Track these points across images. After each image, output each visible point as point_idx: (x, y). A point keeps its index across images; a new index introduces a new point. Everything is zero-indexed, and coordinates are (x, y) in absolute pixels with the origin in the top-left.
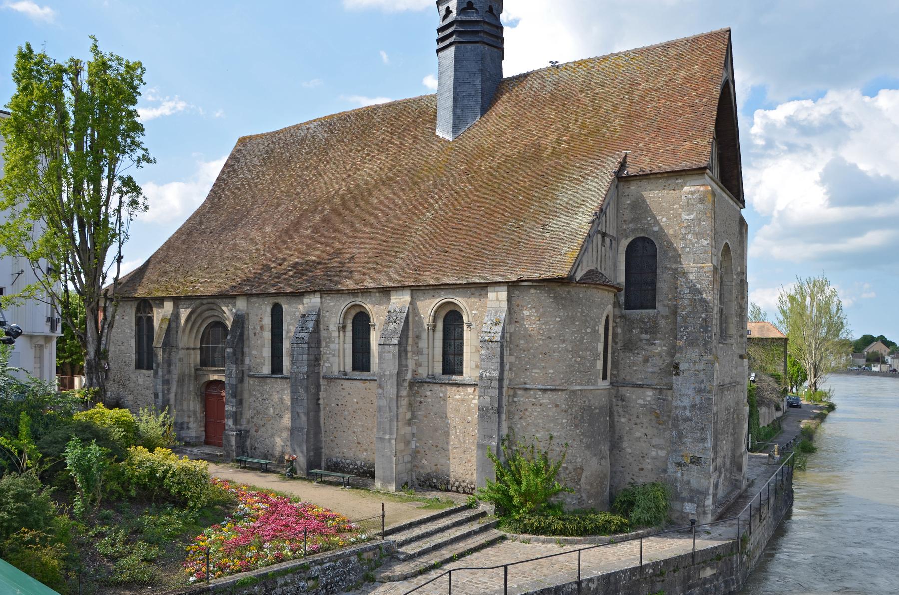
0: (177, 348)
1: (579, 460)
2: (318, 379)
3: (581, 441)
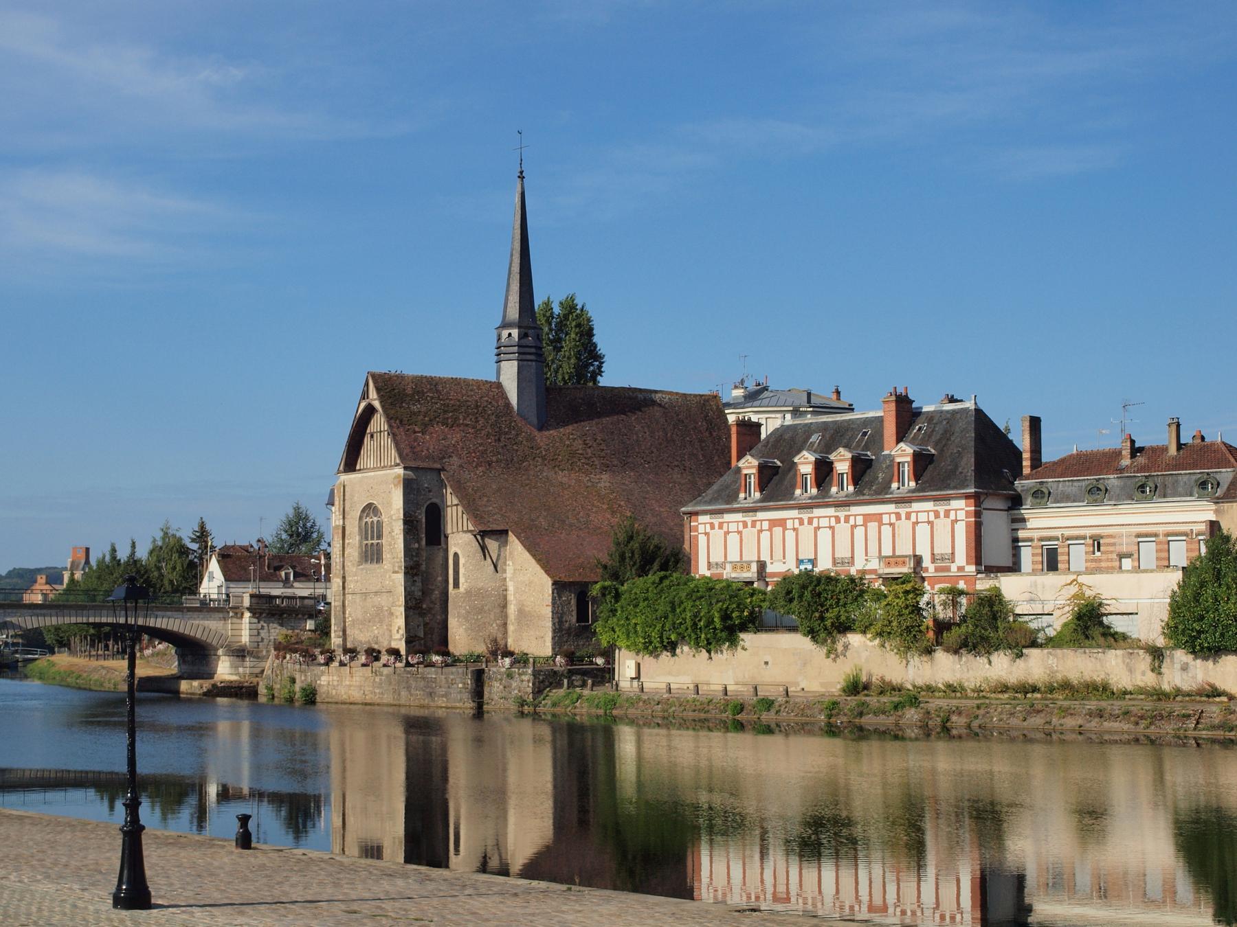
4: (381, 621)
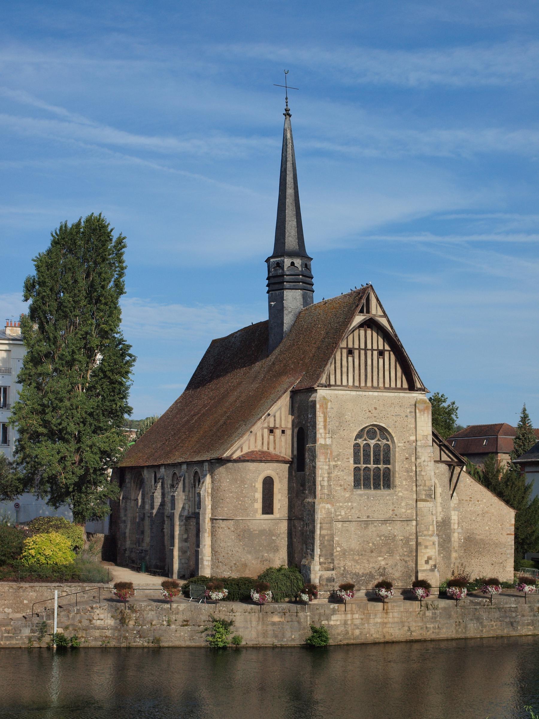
0: (130, 499)
1: (243, 560)
2: (163, 517)
3: (244, 549)
4: (391, 552)
